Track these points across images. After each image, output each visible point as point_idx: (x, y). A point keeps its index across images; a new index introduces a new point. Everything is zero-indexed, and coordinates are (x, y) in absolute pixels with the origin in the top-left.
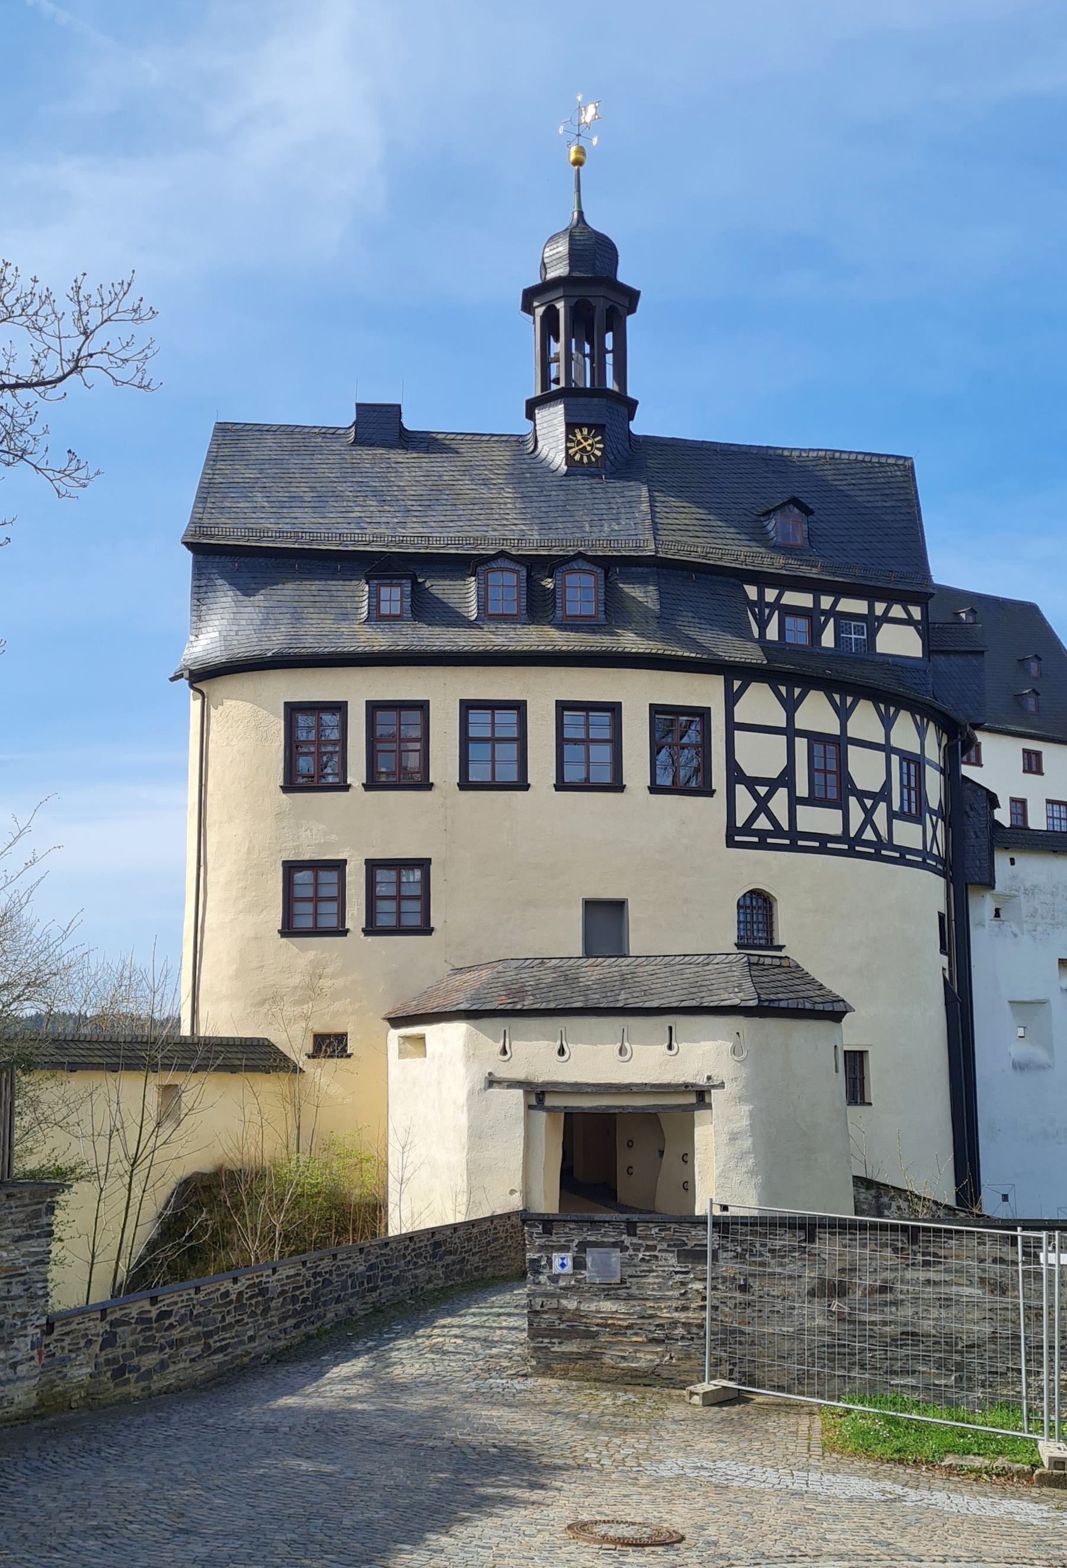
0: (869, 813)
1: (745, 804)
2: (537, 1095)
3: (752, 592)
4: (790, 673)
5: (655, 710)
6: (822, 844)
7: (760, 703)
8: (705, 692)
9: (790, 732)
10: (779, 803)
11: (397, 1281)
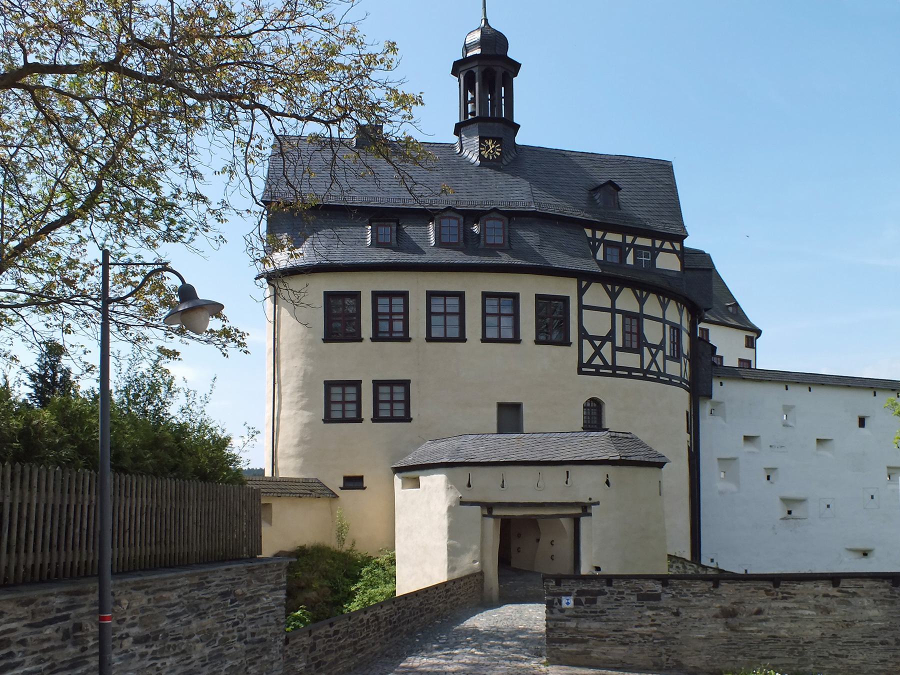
0: (654, 356)
1: (588, 350)
2: (489, 508)
4: (613, 280)
5: (539, 297)
6: (630, 373)
7: (596, 295)
8: (567, 288)
9: (613, 311)
10: (607, 350)
11: (432, 610)
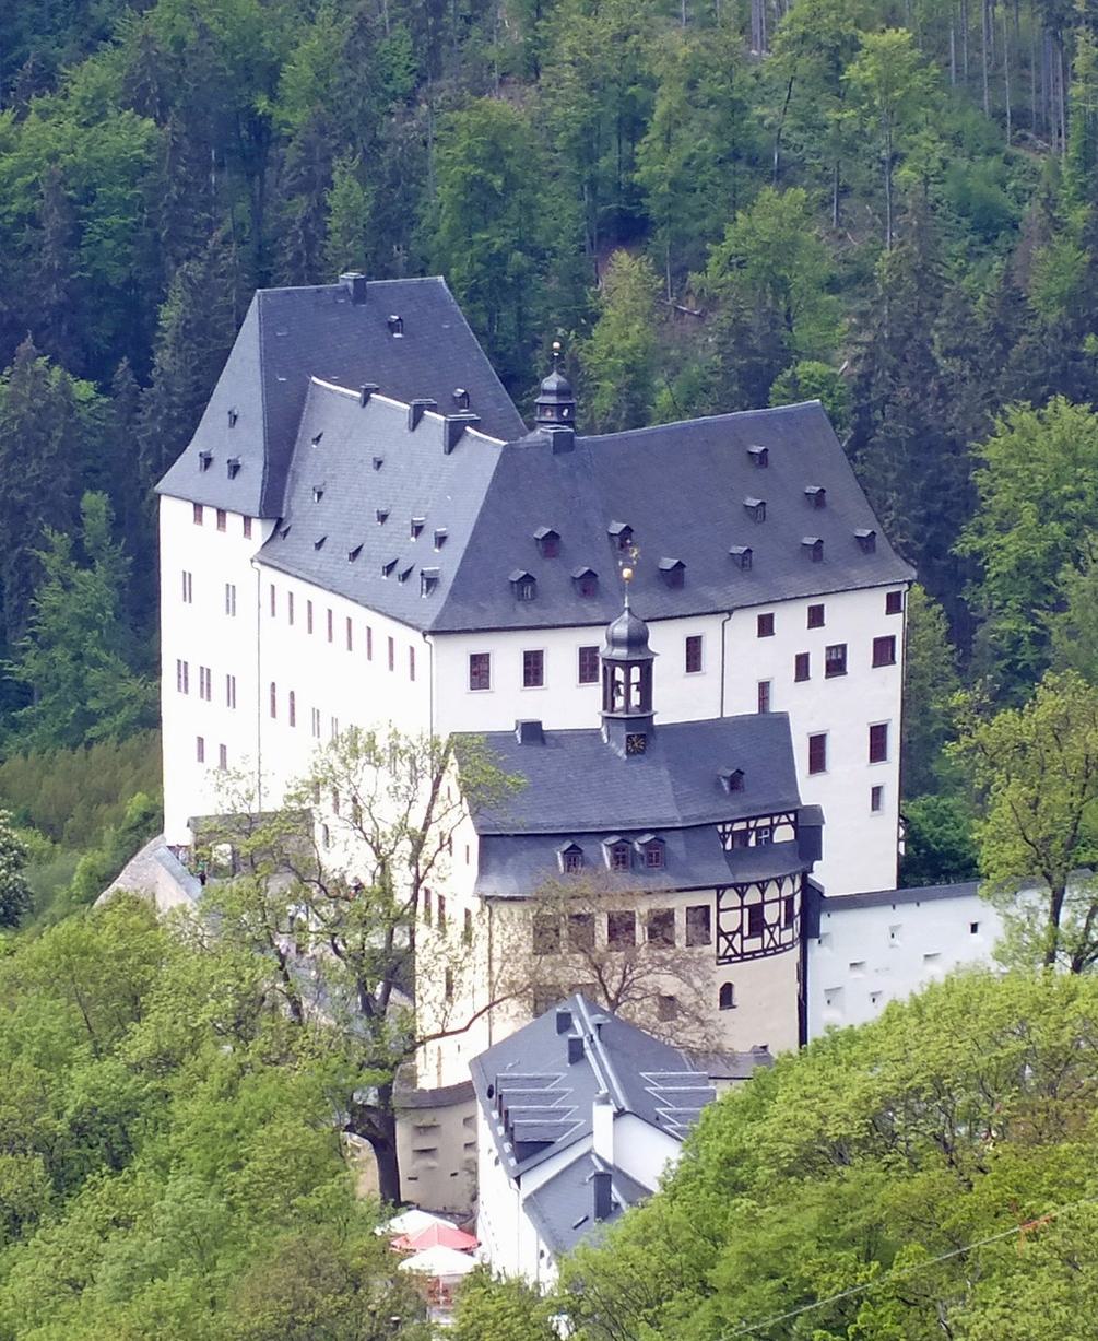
3: (720, 828)
6: (753, 955)
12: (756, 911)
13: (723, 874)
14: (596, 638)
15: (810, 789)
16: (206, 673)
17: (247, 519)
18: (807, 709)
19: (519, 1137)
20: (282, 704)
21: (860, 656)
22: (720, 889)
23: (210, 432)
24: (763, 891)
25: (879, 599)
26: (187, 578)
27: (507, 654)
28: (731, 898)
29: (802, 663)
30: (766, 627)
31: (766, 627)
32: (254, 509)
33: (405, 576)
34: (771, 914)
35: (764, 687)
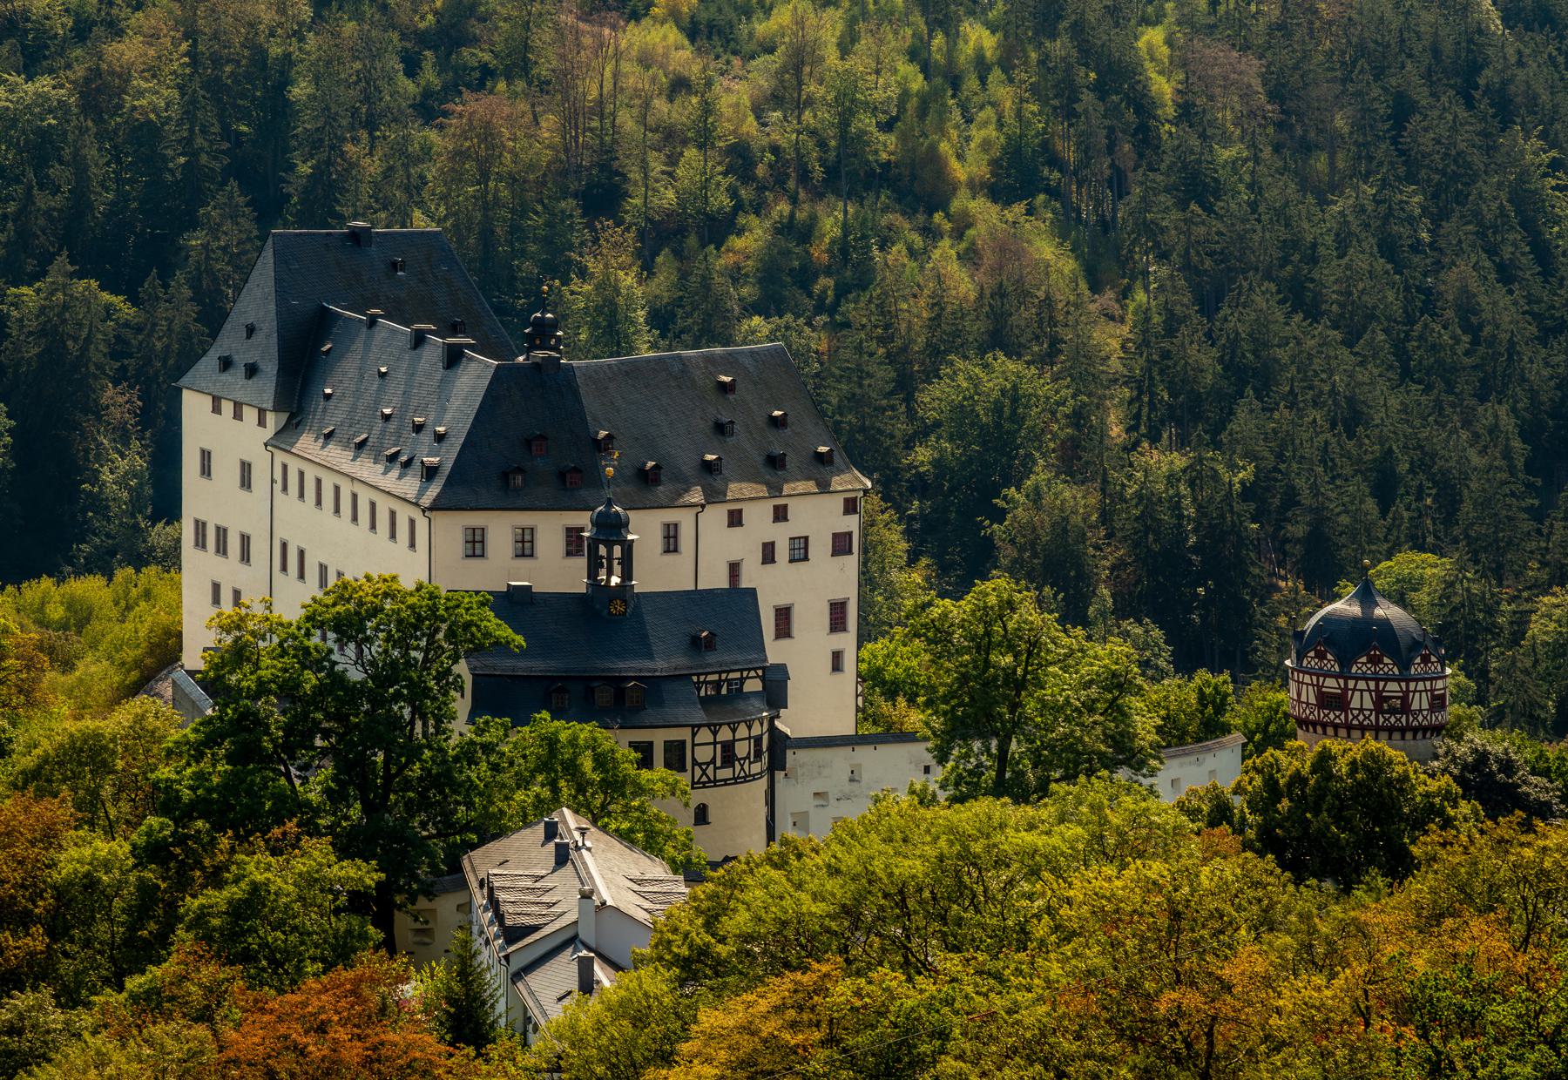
3: (695, 679)
6: (725, 782)
12: (728, 748)
13: (699, 716)
14: (583, 519)
15: (775, 651)
16: (222, 533)
17: (262, 413)
18: (772, 586)
19: (509, 923)
20: (289, 559)
21: (820, 547)
22: (695, 728)
23: (229, 341)
24: (734, 731)
25: (838, 503)
26: (206, 456)
27: (500, 527)
28: (705, 735)
29: (769, 554)
30: (735, 519)
31: (735, 519)
32: (269, 405)
33: (407, 464)
34: (742, 749)
35: (734, 569)
